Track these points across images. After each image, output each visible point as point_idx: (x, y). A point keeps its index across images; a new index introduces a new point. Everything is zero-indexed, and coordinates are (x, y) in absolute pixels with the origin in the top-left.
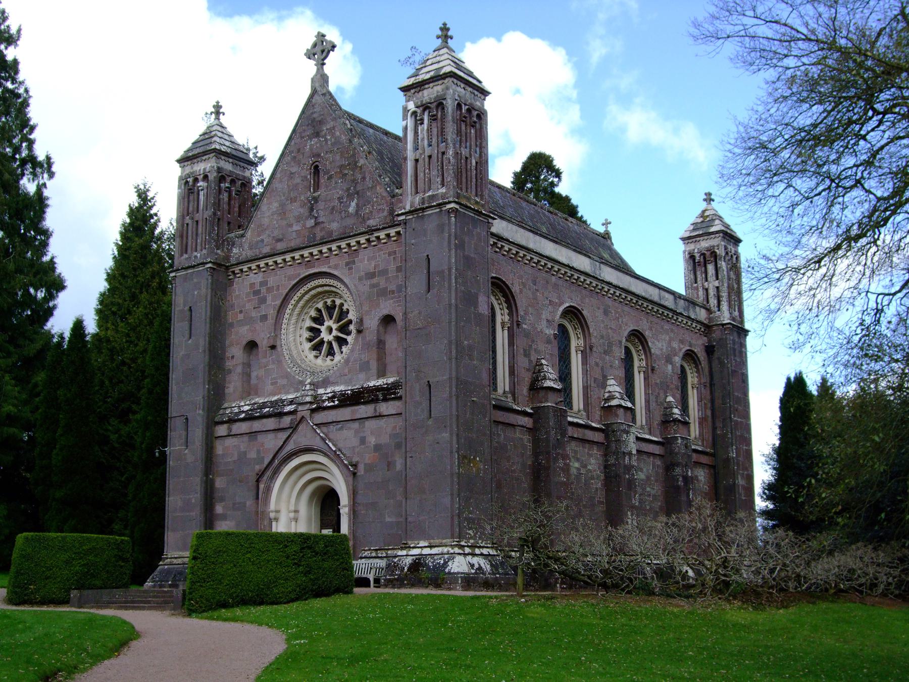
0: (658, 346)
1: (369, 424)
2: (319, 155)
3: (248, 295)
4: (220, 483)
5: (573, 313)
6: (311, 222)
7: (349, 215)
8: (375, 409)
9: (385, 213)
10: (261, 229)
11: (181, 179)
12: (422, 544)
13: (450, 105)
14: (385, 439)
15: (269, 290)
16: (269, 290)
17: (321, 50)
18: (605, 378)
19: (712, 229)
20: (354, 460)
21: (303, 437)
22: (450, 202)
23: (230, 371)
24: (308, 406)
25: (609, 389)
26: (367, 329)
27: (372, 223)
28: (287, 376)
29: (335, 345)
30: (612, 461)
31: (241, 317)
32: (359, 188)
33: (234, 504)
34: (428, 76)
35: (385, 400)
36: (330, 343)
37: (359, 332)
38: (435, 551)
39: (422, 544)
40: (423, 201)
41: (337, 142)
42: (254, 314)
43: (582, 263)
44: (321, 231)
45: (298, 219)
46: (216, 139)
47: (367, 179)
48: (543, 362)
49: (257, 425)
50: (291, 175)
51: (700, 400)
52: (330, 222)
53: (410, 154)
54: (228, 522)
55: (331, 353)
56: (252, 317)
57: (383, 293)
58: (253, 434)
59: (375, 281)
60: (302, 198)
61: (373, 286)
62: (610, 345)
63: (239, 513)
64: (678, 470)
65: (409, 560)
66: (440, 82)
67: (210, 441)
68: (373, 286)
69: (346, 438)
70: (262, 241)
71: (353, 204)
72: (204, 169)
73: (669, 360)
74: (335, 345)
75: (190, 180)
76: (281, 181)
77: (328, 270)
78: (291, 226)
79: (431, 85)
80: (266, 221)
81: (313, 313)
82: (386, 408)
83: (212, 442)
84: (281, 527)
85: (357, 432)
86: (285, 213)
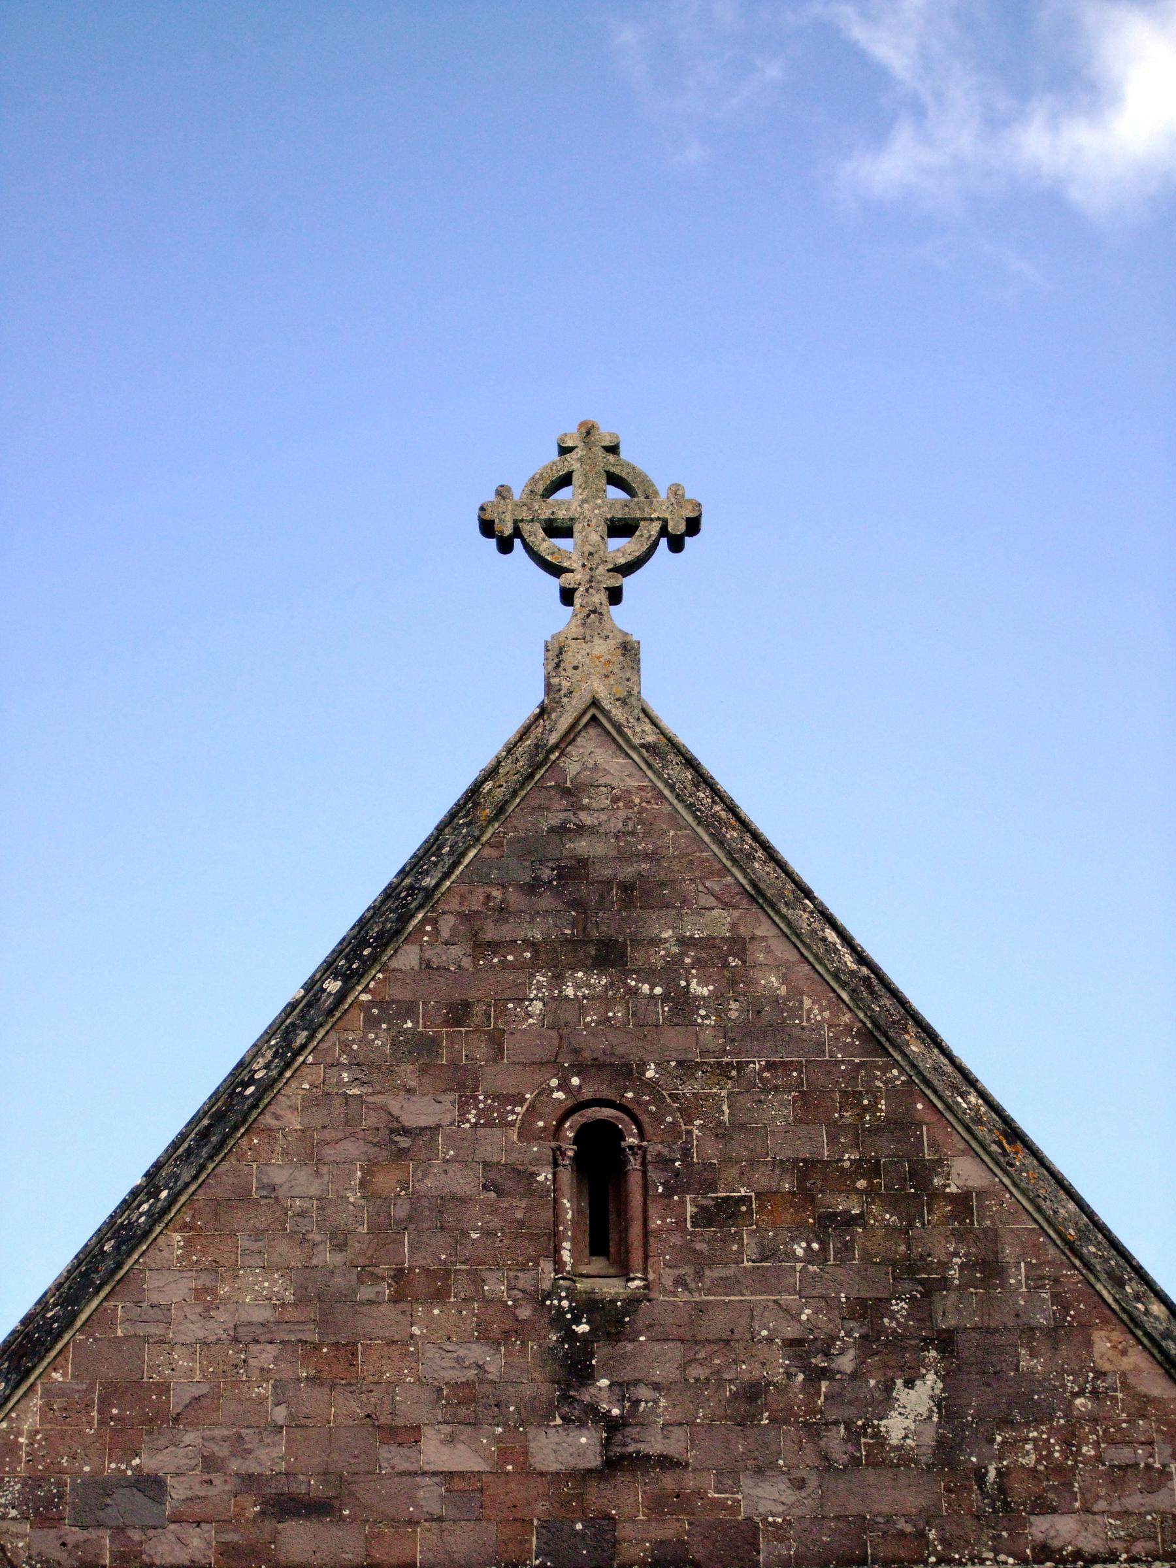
2: (627, 1072)
6: (585, 1445)
7: (878, 1456)
17: (595, 521)
32: (951, 1312)
41: (767, 1023)
44: (658, 1505)
45: (467, 1404)
47: (1018, 1277)
50: (401, 1143)
52: (729, 1474)
60: (495, 1286)
76: (311, 1154)
78: (411, 1435)
80: (183, 1374)
86: (348, 1351)
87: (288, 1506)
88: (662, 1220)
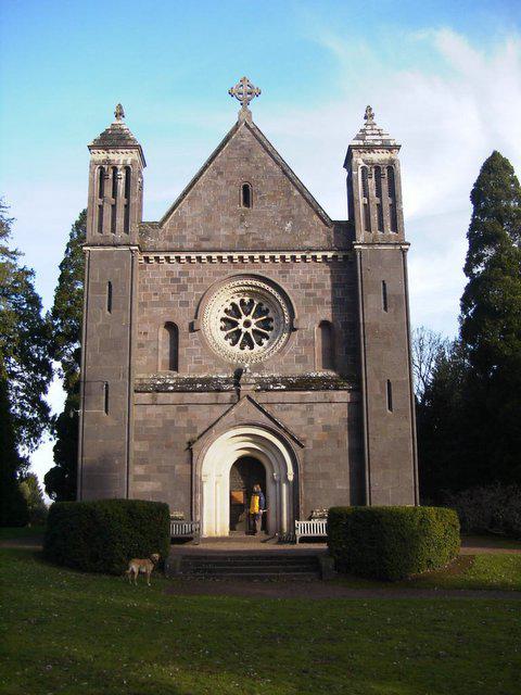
1: (319, 408)
2: (250, 178)
3: (164, 280)
11: (94, 163)
16: (189, 280)
17: (246, 94)
20: (303, 436)
24: (252, 387)
28: (214, 357)
31: (154, 299)
32: (295, 212)
33: (158, 468)
35: (337, 389)
36: (239, 332)
42: (172, 299)
49: (188, 397)
54: (151, 483)
59: (312, 290)
61: (307, 294)
63: (167, 475)
68: (307, 294)
69: (292, 419)
77: (261, 274)
87: (203, 239)
88: (255, 199)
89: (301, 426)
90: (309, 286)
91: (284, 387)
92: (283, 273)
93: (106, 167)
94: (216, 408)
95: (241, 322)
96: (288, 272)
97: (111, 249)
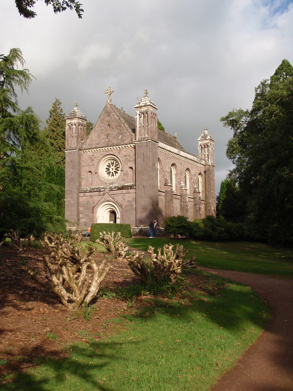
0: (193, 172)
3: (88, 158)
4: (81, 209)
5: (173, 165)
7: (119, 139)
8: (128, 191)
9: (130, 140)
10: (92, 141)
12: (142, 226)
13: (149, 113)
14: (130, 199)
15: (95, 157)
16: (95, 157)
18: (181, 182)
19: (207, 138)
20: (122, 204)
21: (107, 197)
22: (149, 140)
23: (83, 179)
25: (181, 184)
26: (124, 170)
27: (126, 142)
28: (101, 181)
29: (114, 173)
30: (182, 204)
34: (143, 105)
35: (131, 189)
37: (122, 171)
38: (145, 227)
39: (142, 226)
40: (141, 138)
41: (115, 119)
42: (90, 164)
43: (176, 151)
44: (111, 143)
45: (104, 139)
46: (77, 114)
48: (167, 178)
49: (92, 194)
50: (101, 126)
51: (202, 186)
53: (138, 125)
55: (113, 175)
56: (89, 165)
57: (129, 161)
58: (91, 196)
61: (126, 159)
62: (182, 172)
64: (197, 206)
65: (138, 230)
66: (146, 107)
67: (78, 197)
68: (126, 159)
69: (119, 199)
70: (93, 144)
71: (120, 136)
72: (74, 122)
73: (195, 176)
74: (114, 173)
75: (70, 125)
77: (113, 154)
79: (144, 107)
80: (94, 139)
81: (108, 164)
82: (131, 191)
83: (79, 198)
84: (99, 221)
85: (122, 197)
89: (122, 201)
90: (126, 156)
91: (117, 189)
92: (119, 152)
93: (70, 125)
94: (100, 196)
95: (111, 169)
96: (120, 152)
97: (72, 151)
